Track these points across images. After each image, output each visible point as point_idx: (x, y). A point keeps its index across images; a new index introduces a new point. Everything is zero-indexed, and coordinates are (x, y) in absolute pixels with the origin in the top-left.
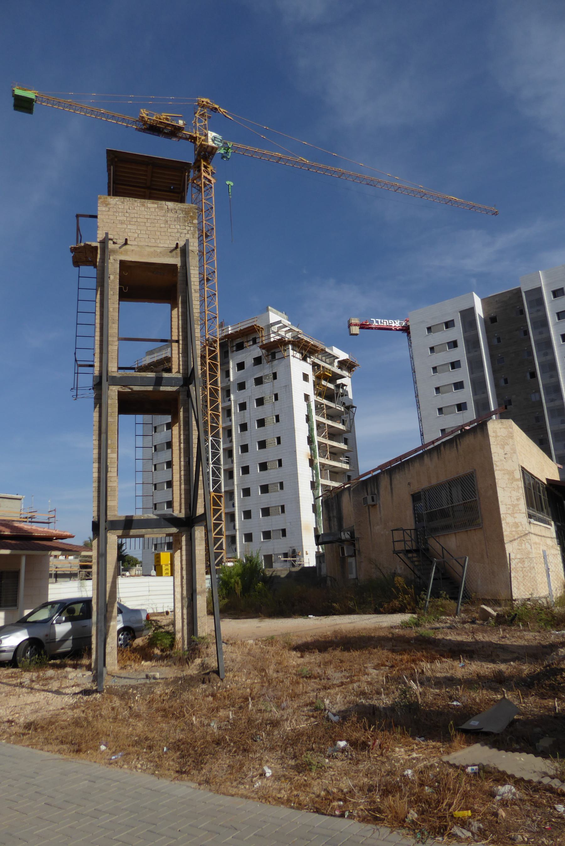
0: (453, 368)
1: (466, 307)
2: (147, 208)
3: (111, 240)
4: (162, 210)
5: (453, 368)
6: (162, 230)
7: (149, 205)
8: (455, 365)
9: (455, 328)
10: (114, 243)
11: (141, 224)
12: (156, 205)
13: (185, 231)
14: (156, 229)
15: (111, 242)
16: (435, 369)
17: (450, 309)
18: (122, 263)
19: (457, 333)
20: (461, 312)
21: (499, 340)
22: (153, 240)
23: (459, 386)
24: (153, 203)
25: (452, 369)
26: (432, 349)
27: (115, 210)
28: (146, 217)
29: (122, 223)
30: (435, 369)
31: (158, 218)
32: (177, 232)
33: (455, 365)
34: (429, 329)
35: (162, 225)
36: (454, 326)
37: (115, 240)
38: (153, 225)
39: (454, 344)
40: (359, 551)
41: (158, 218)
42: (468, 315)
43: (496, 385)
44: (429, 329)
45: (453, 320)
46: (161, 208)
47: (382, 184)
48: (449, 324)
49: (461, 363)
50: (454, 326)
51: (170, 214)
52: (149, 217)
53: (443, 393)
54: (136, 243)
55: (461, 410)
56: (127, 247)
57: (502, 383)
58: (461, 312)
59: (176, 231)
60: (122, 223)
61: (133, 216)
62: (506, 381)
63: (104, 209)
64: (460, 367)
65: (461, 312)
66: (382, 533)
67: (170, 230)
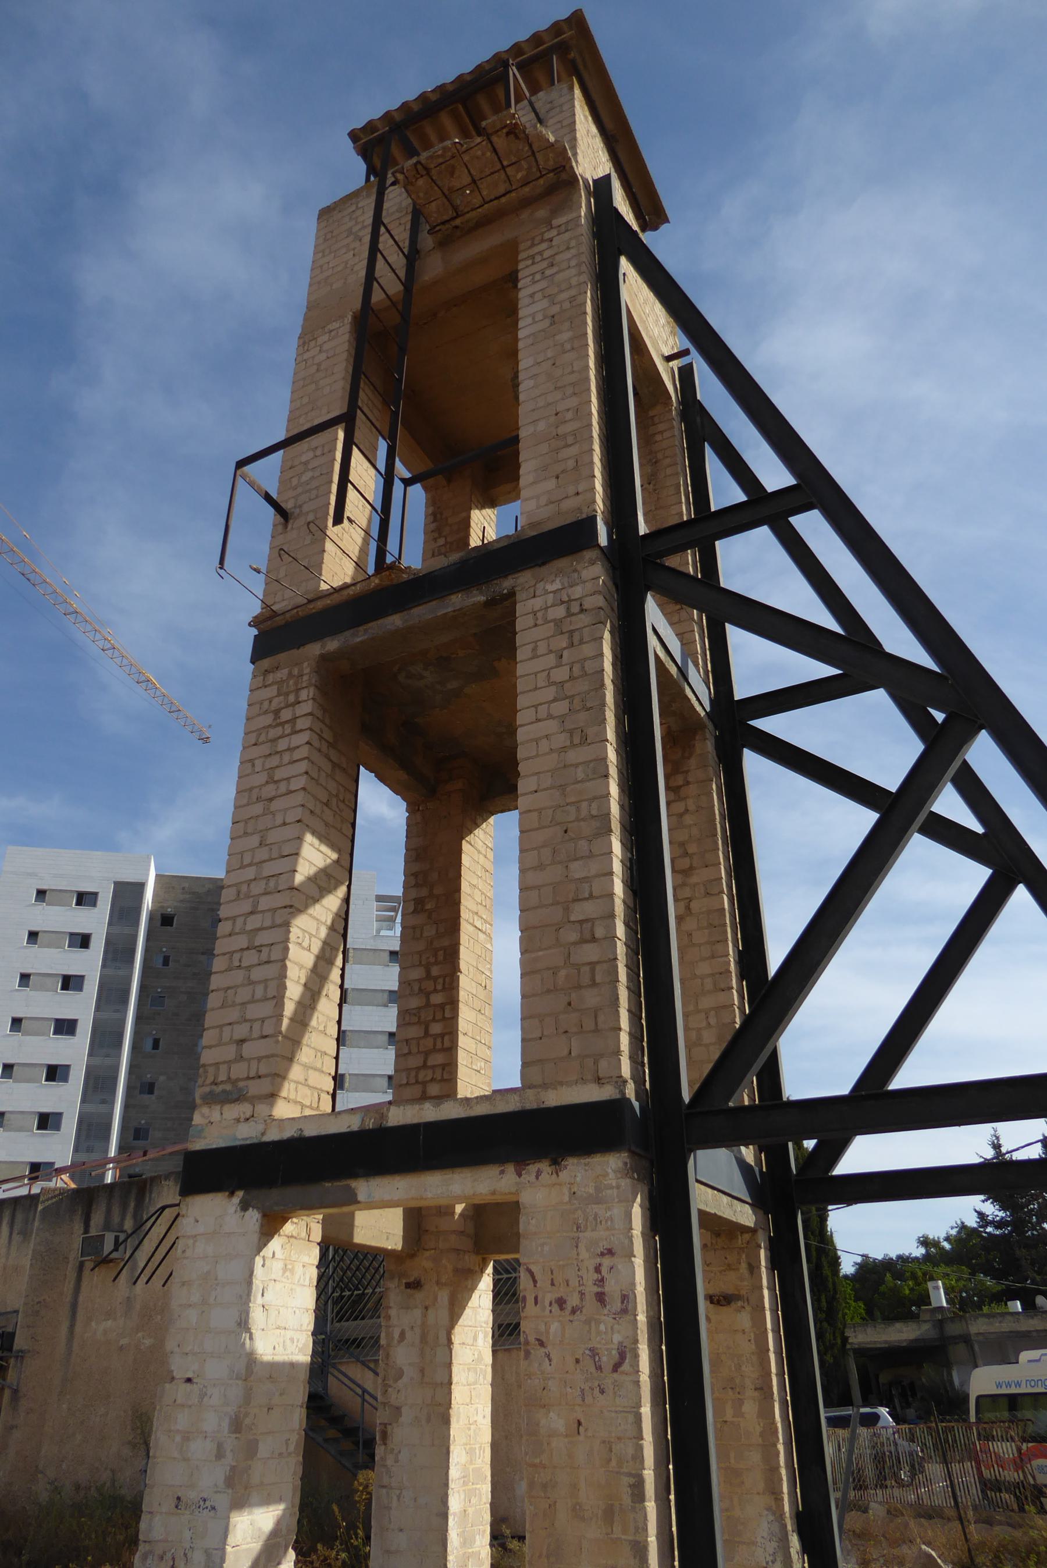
0: (65, 987)
1: (129, 876)
5: (65, 987)
8: (70, 983)
9: (96, 910)
16: (25, 978)
17: (99, 873)
19: (96, 921)
20: (117, 884)
21: (166, 961)
23: (66, 1027)
25: (63, 989)
26: (33, 936)
30: (25, 978)
33: (70, 983)
34: (41, 894)
36: (94, 905)
39: (83, 941)
40: (15, 1392)
42: (128, 895)
43: (135, 1047)
44: (41, 894)
45: (96, 894)
47: (49, 590)
48: (85, 899)
49: (86, 982)
50: (94, 905)
53: (27, 1033)
55: (53, 1080)
57: (149, 1044)
58: (116, 884)
62: (156, 1044)
64: (81, 989)
65: (116, 884)
66: (124, 1341)
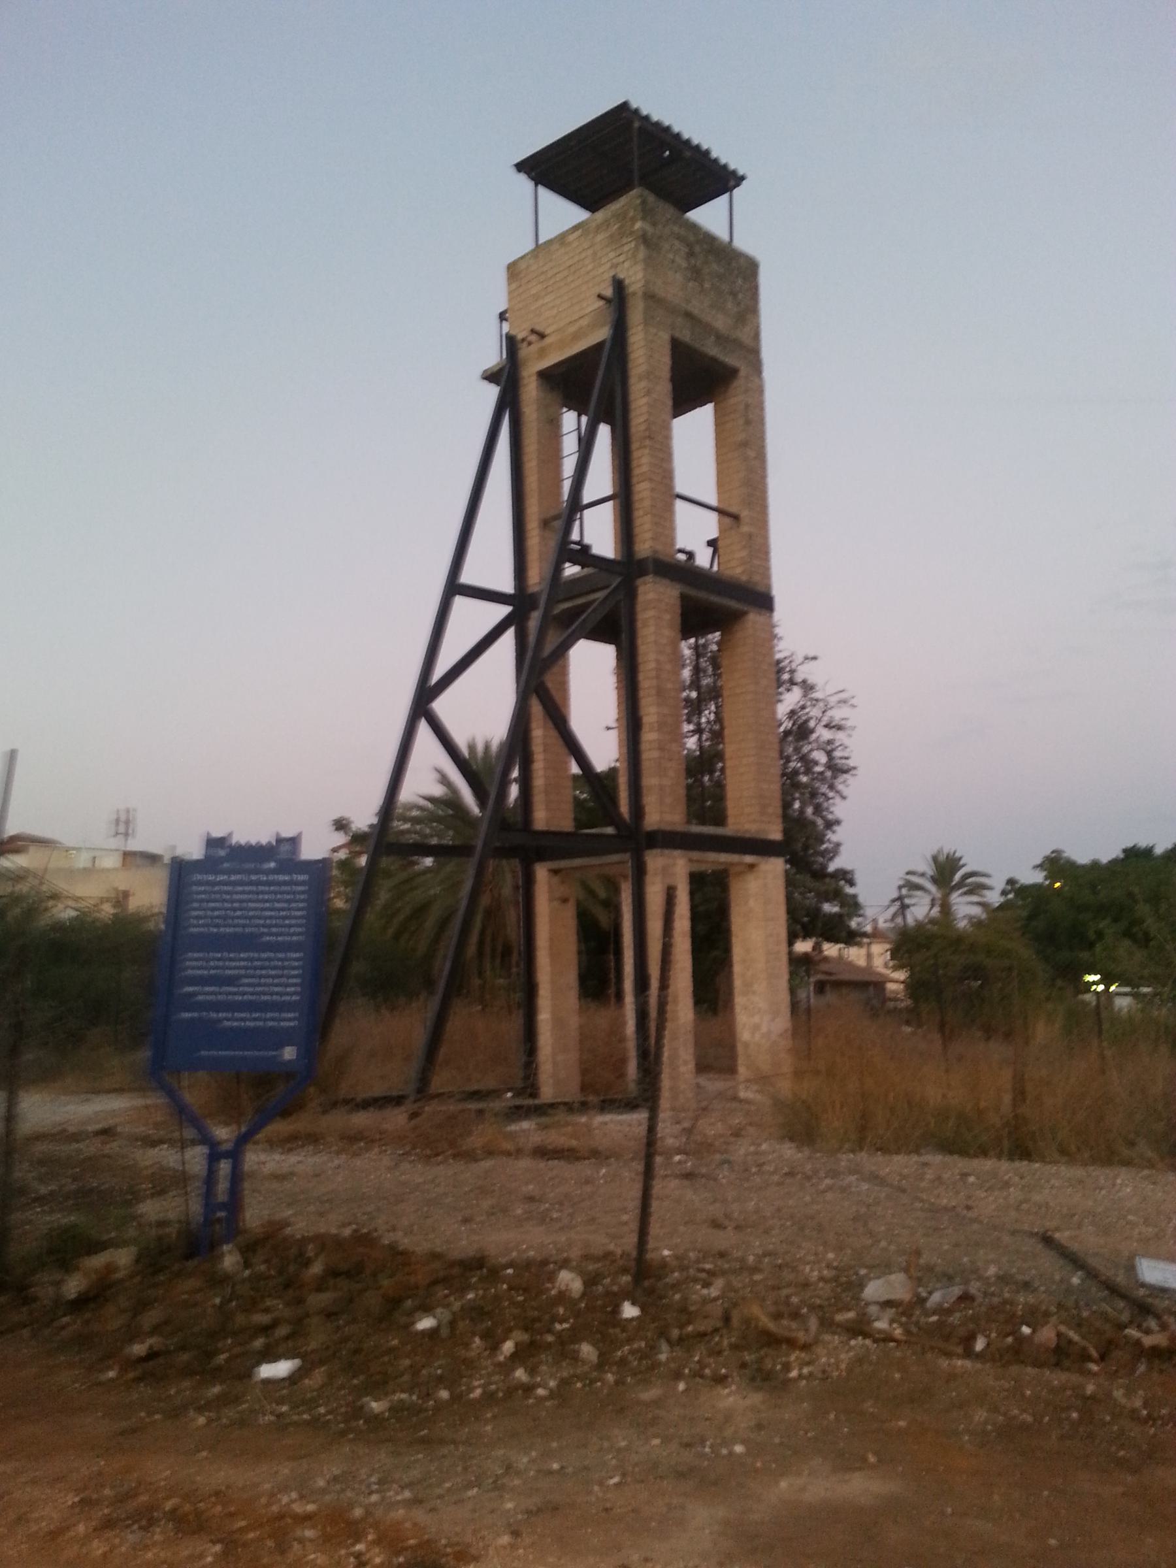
3: (523, 340)
13: (622, 258)
15: (525, 344)
18: (544, 375)
29: (537, 297)
31: (583, 255)
35: (590, 267)
41: (583, 255)
51: (600, 237)
54: (554, 327)
56: (547, 341)
59: (609, 265)
60: (537, 297)
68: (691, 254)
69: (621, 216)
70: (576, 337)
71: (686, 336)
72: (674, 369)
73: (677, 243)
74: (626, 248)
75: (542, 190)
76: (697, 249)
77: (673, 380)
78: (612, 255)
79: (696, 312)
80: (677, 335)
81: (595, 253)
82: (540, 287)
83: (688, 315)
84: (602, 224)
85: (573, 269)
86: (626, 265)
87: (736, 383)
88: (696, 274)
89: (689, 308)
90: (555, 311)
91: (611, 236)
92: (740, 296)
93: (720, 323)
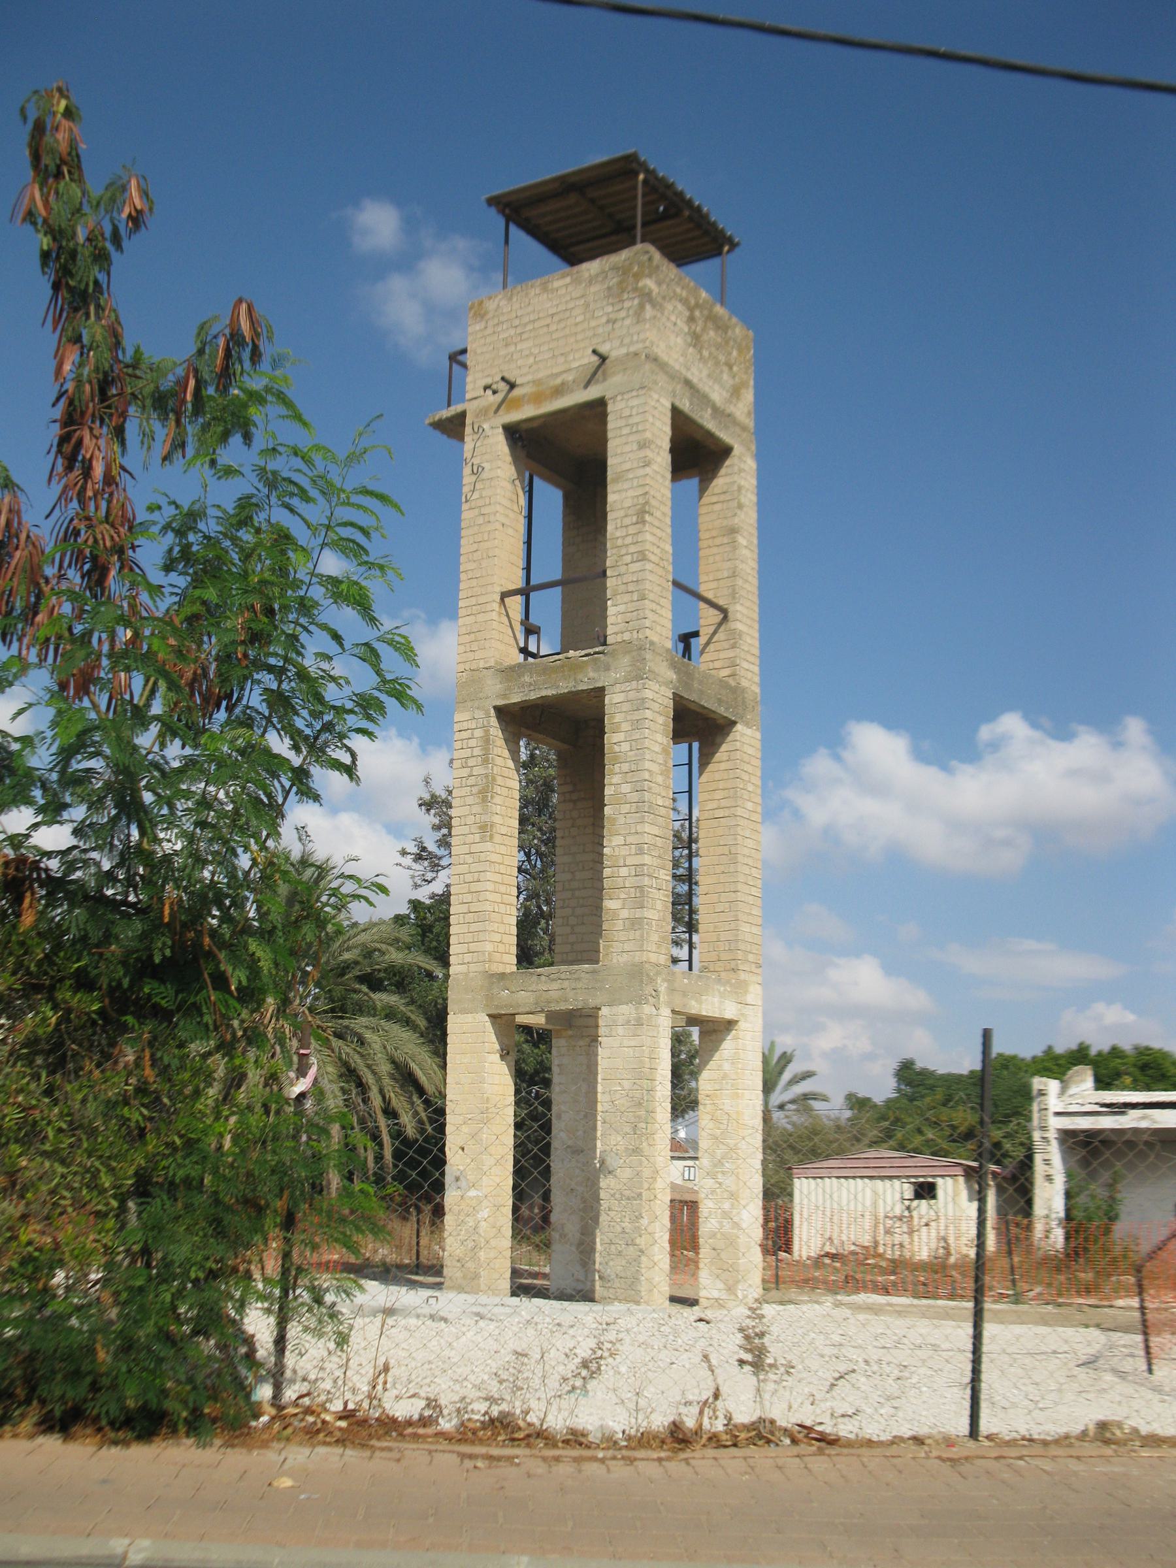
2: (552, 290)
4: (580, 283)
6: (579, 328)
7: (556, 284)
10: (495, 392)
11: (541, 332)
12: (568, 280)
13: (623, 314)
14: (567, 331)
22: (561, 360)
24: (563, 277)
27: (496, 321)
28: (550, 312)
32: (608, 321)
35: (579, 319)
37: (494, 387)
38: (562, 325)
46: (577, 281)
52: (554, 310)
54: (530, 378)
56: (516, 392)
59: (604, 320)
61: (526, 319)
63: (478, 327)
67: (593, 323)
68: (691, 319)
69: (624, 270)
70: (559, 391)
71: (685, 405)
72: (673, 441)
73: (680, 306)
74: (627, 304)
75: (513, 228)
76: (697, 313)
77: (672, 451)
78: (610, 309)
79: (695, 381)
80: (677, 403)
81: (587, 305)
82: (512, 332)
83: (688, 383)
84: (597, 275)
85: (556, 318)
86: (628, 322)
87: (727, 463)
88: (696, 340)
89: (689, 376)
90: (531, 360)
91: (609, 288)
92: (735, 369)
93: (717, 395)
